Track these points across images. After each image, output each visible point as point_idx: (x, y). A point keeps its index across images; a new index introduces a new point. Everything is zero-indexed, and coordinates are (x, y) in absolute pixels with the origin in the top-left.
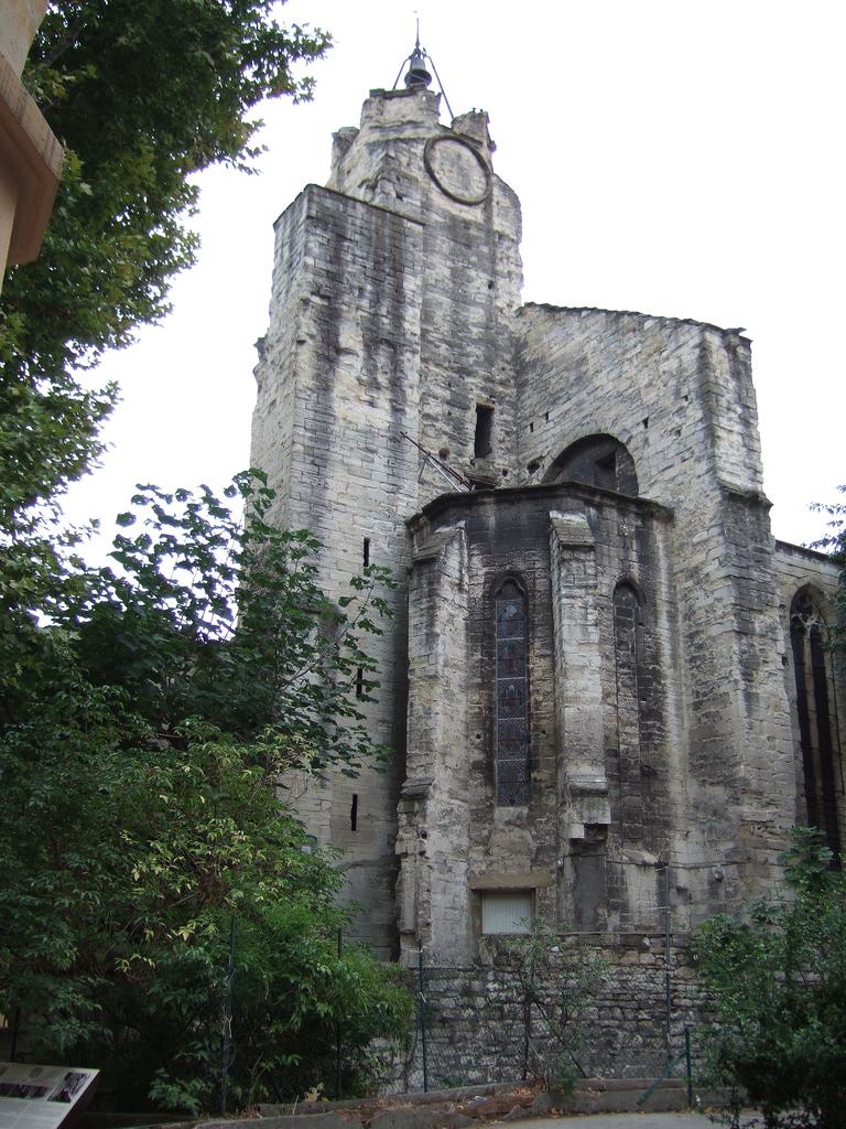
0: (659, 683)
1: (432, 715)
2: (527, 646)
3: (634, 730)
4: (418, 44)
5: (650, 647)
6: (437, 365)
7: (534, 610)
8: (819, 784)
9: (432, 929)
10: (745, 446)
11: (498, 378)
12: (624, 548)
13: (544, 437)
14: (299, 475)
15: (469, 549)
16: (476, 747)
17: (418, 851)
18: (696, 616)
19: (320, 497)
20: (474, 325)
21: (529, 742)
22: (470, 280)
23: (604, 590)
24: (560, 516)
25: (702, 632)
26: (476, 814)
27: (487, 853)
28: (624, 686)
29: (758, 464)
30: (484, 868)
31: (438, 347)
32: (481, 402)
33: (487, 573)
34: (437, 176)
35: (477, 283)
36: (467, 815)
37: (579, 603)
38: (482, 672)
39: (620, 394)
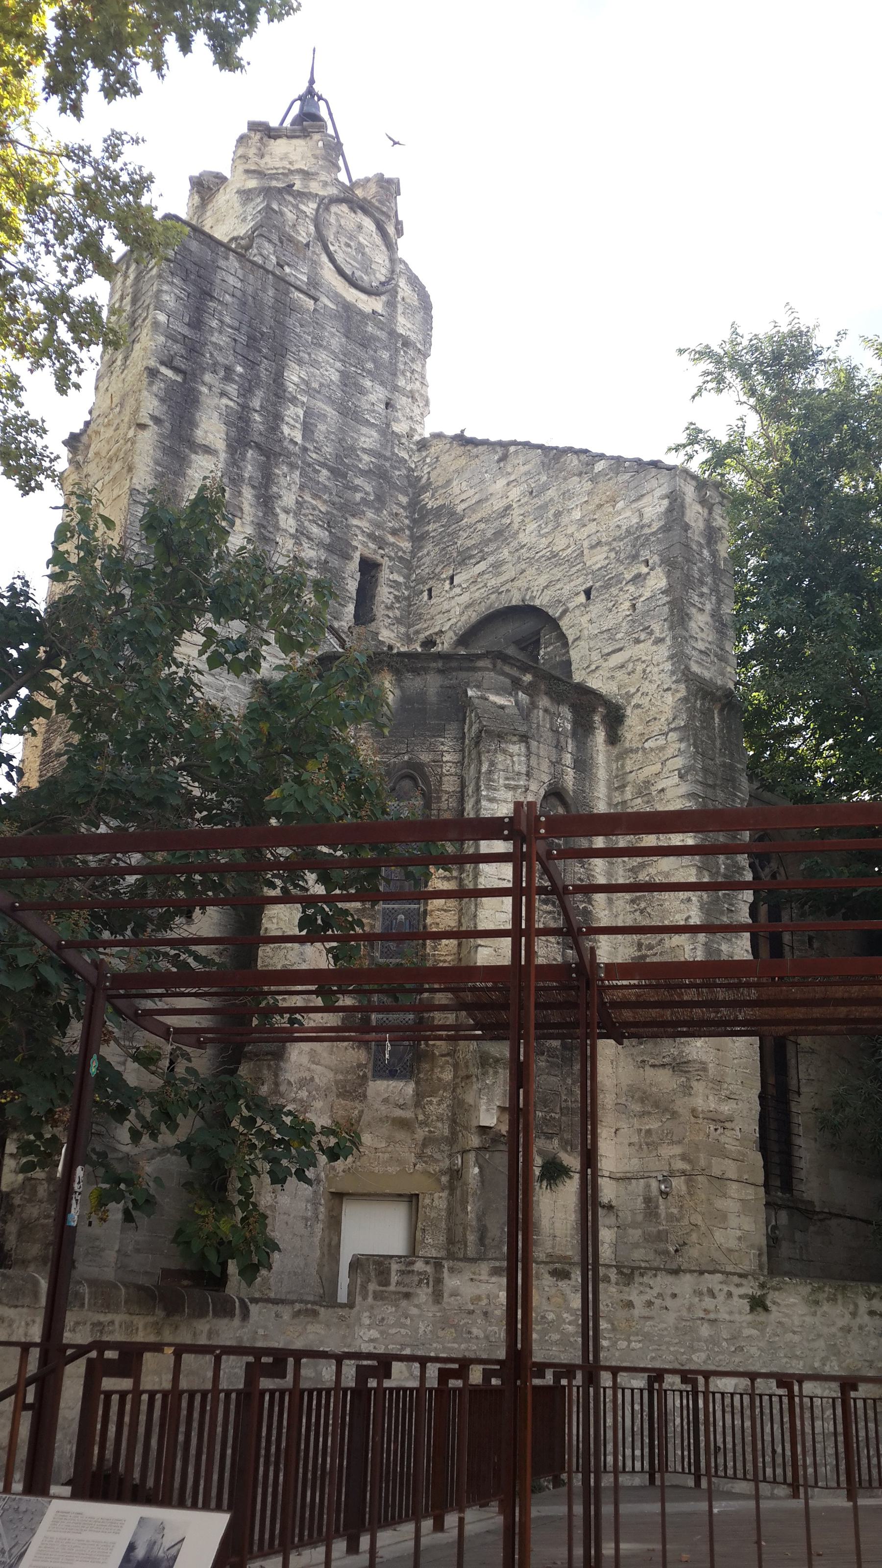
12: (556, 747)
20: (364, 450)
22: (363, 391)
32: (368, 553)
34: (332, 248)
35: (372, 398)
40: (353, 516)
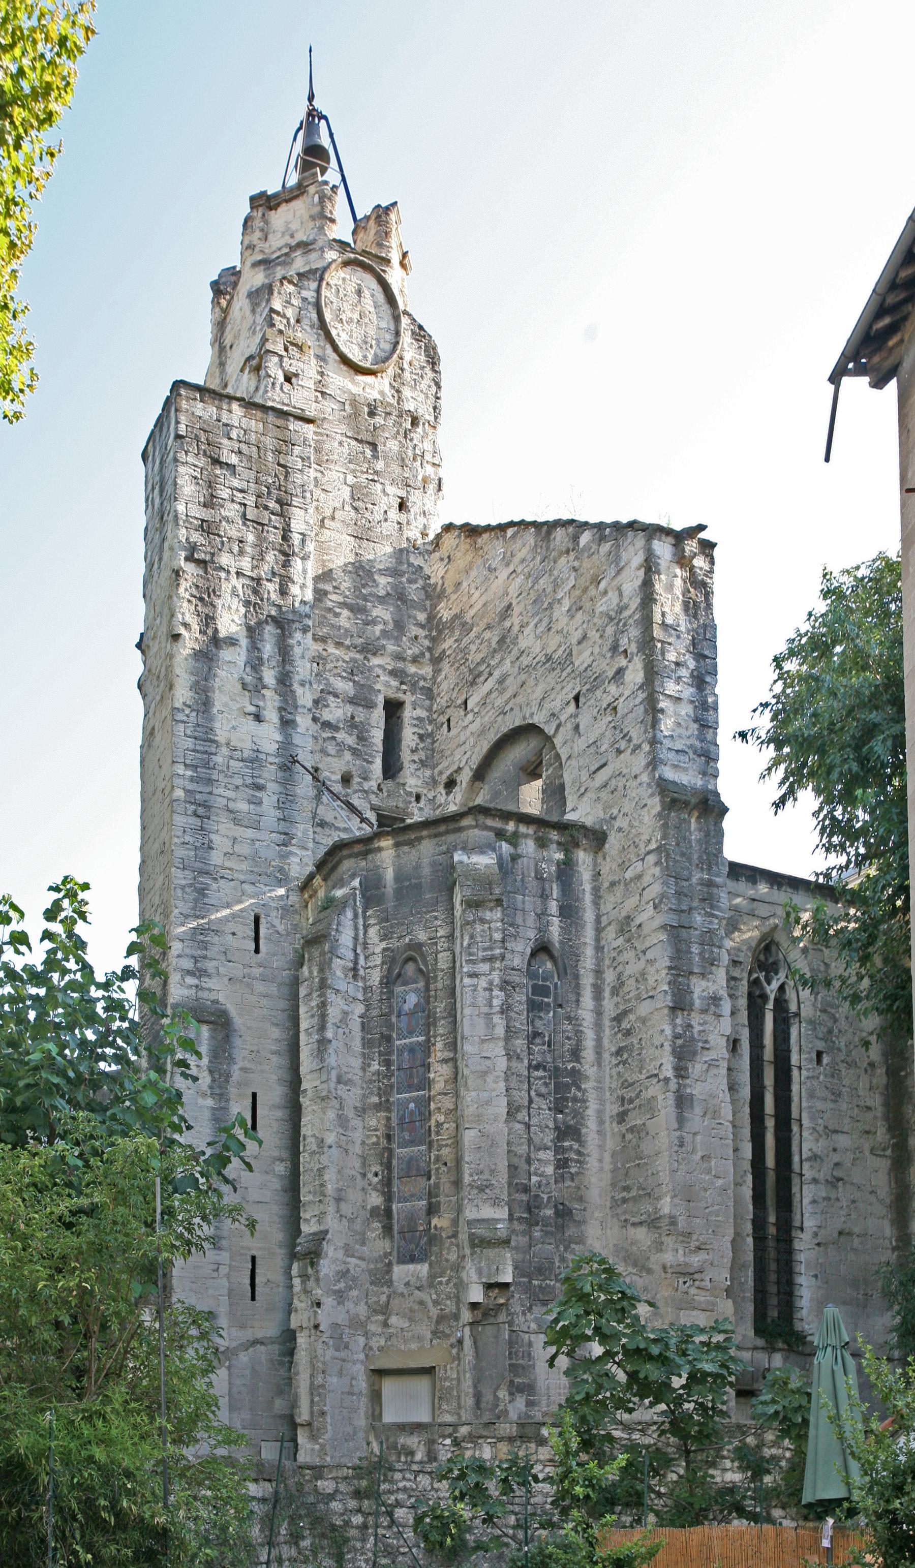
0: (579, 1088)
1: (326, 1149)
2: (427, 1047)
3: (548, 1155)
4: (311, 98)
5: (569, 1038)
6: (338, 644)
7: (436, 997)
8: (772, 1219)
9: (328, 1419)
10: (696, 720)
11: (410, 652)
13: (463, 738)
14: (180, 833)
15: (365, 918)
16: (375, 1189)
17: (312, 1324)
18: (626, 989)
19: (204, 861)
21: (429, 1178)
23: (517, 962)
24: (465, 858)
25: (630, 1011)
26: (375, 1275)
27: (385, 1324)
28: (539, 1095)
29: (712, 748)
30: (382, 1342)
31: (337, 615)
32: (392, 694)
33: (385, 950)
36: (366, 1277)
37: (483, 983)
38: (379, 1089)
39: (549, 658)
40: (374, 654)
